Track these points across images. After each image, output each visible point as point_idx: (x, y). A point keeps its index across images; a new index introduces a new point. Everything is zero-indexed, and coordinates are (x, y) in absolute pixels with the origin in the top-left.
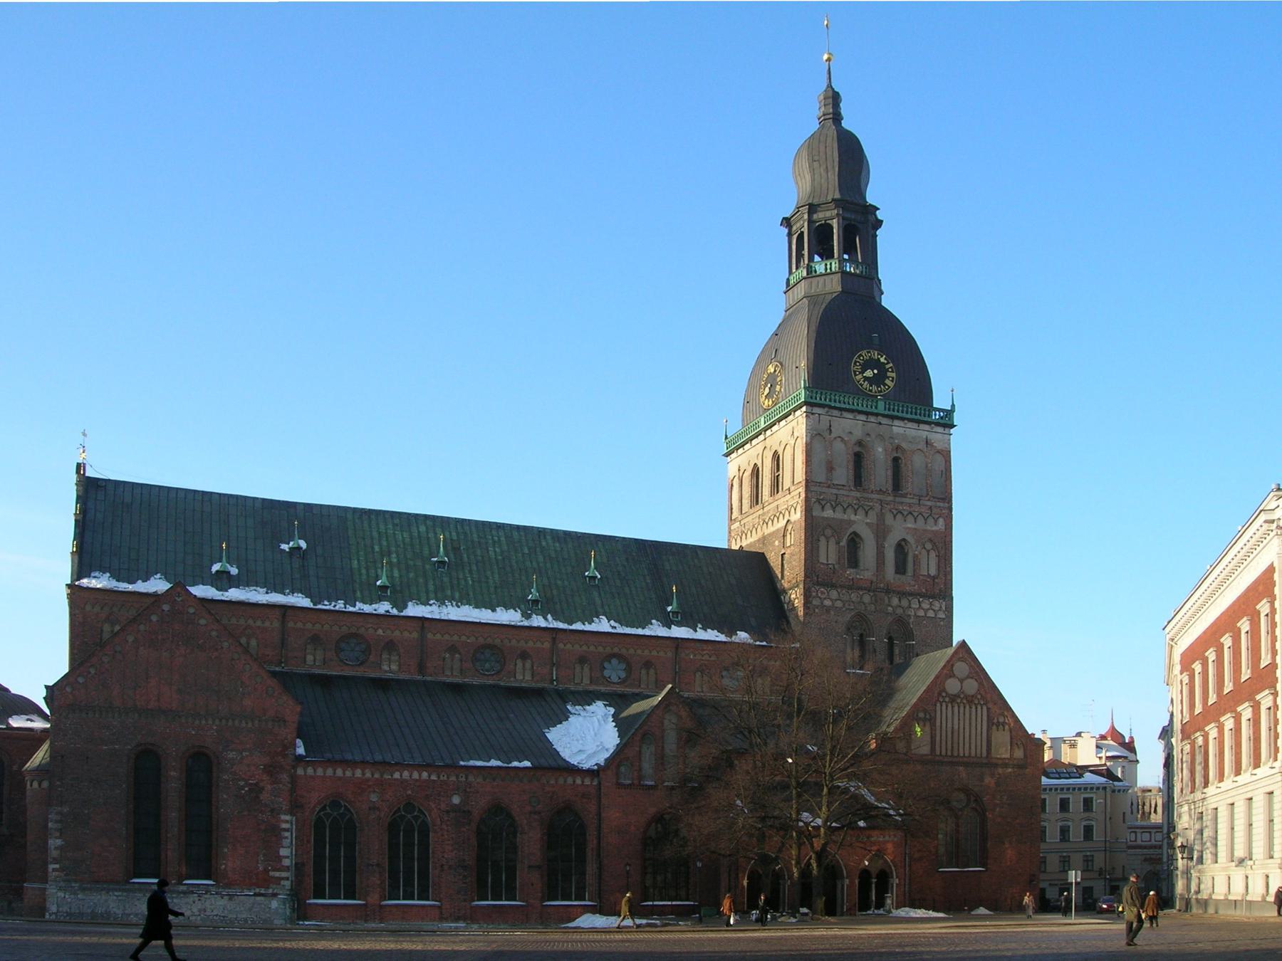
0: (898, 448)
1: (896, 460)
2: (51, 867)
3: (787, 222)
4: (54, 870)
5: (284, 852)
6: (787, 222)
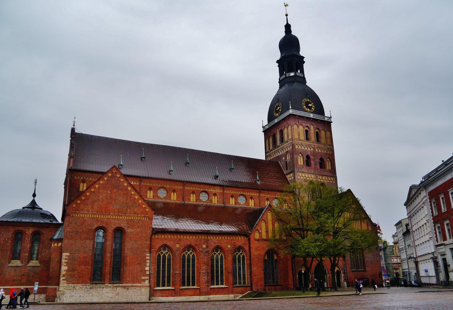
1: (317, 132)
2: (62, 278)
3: (278, 62)
4: (63, 280)
6: (278, 62)
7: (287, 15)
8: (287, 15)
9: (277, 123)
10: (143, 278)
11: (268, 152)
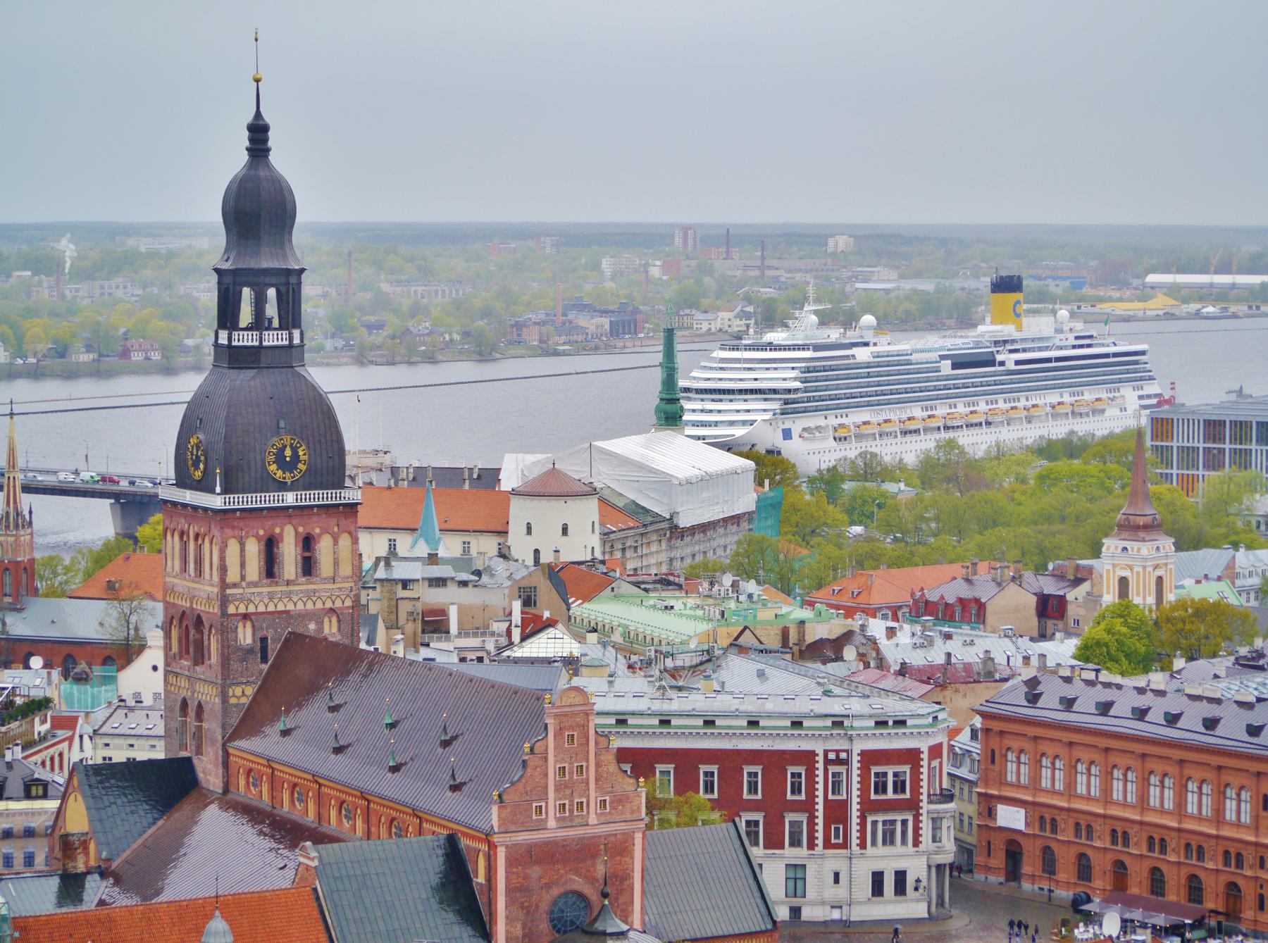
7: (257, 81)
8: (257, 81)
9: (294, 508)
11: (235, 585)
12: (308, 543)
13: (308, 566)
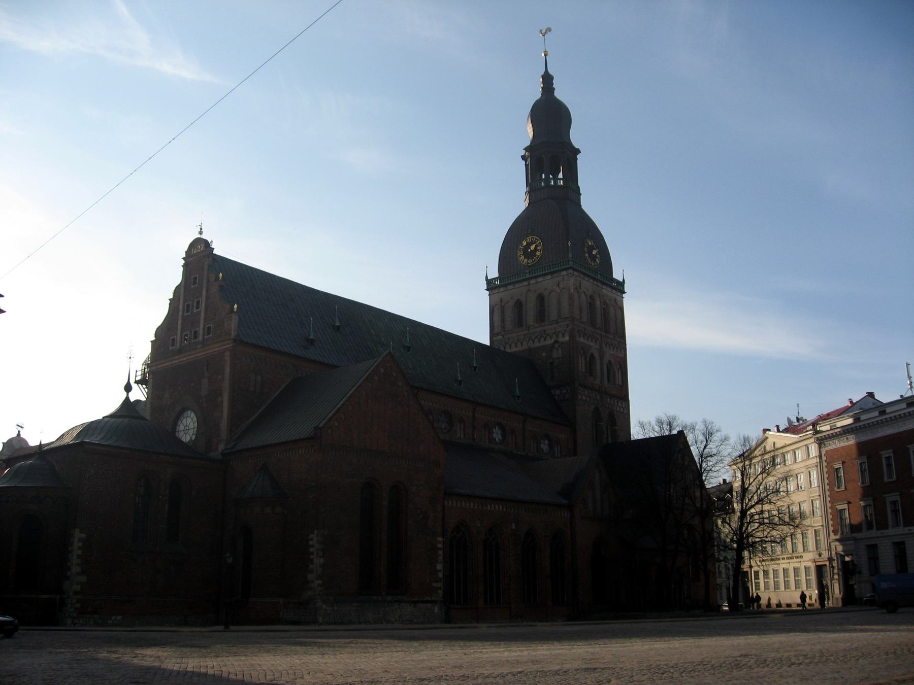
0: (605, 303)
4: (319, 585)
5: (439, 567)
10: (435, 585)
11: (497, 334)
12: (541, 299)
13: (541, 315)
